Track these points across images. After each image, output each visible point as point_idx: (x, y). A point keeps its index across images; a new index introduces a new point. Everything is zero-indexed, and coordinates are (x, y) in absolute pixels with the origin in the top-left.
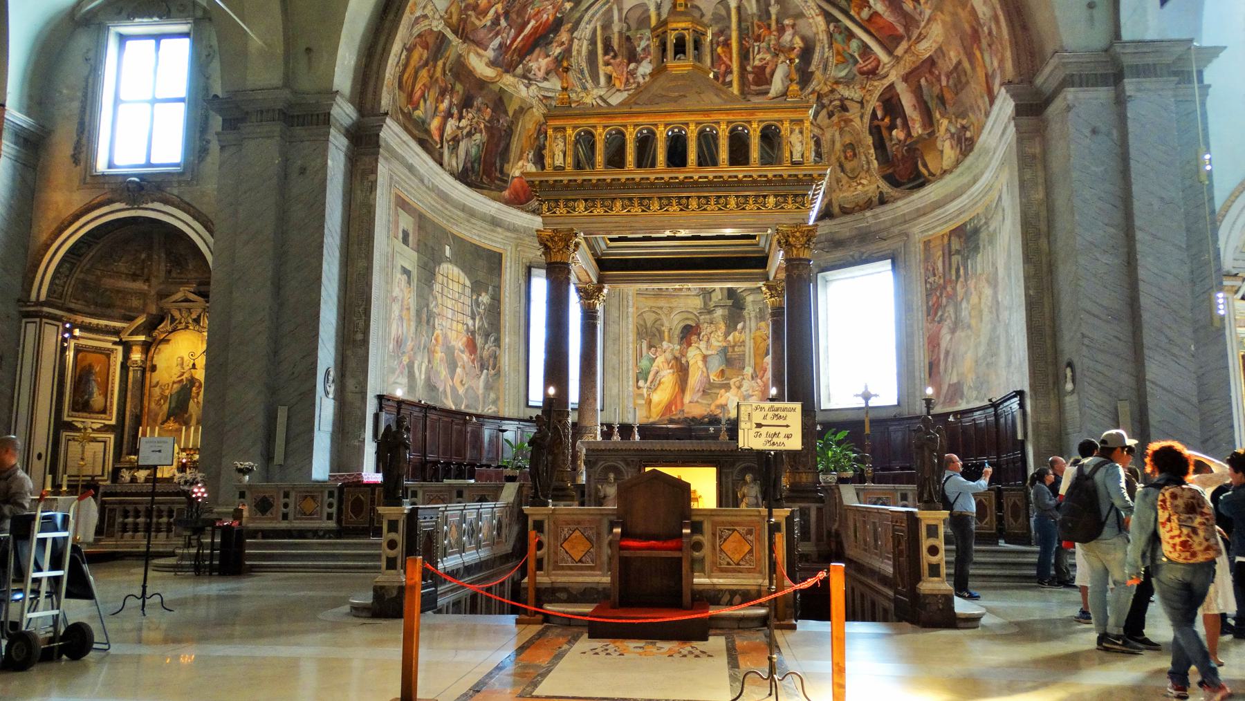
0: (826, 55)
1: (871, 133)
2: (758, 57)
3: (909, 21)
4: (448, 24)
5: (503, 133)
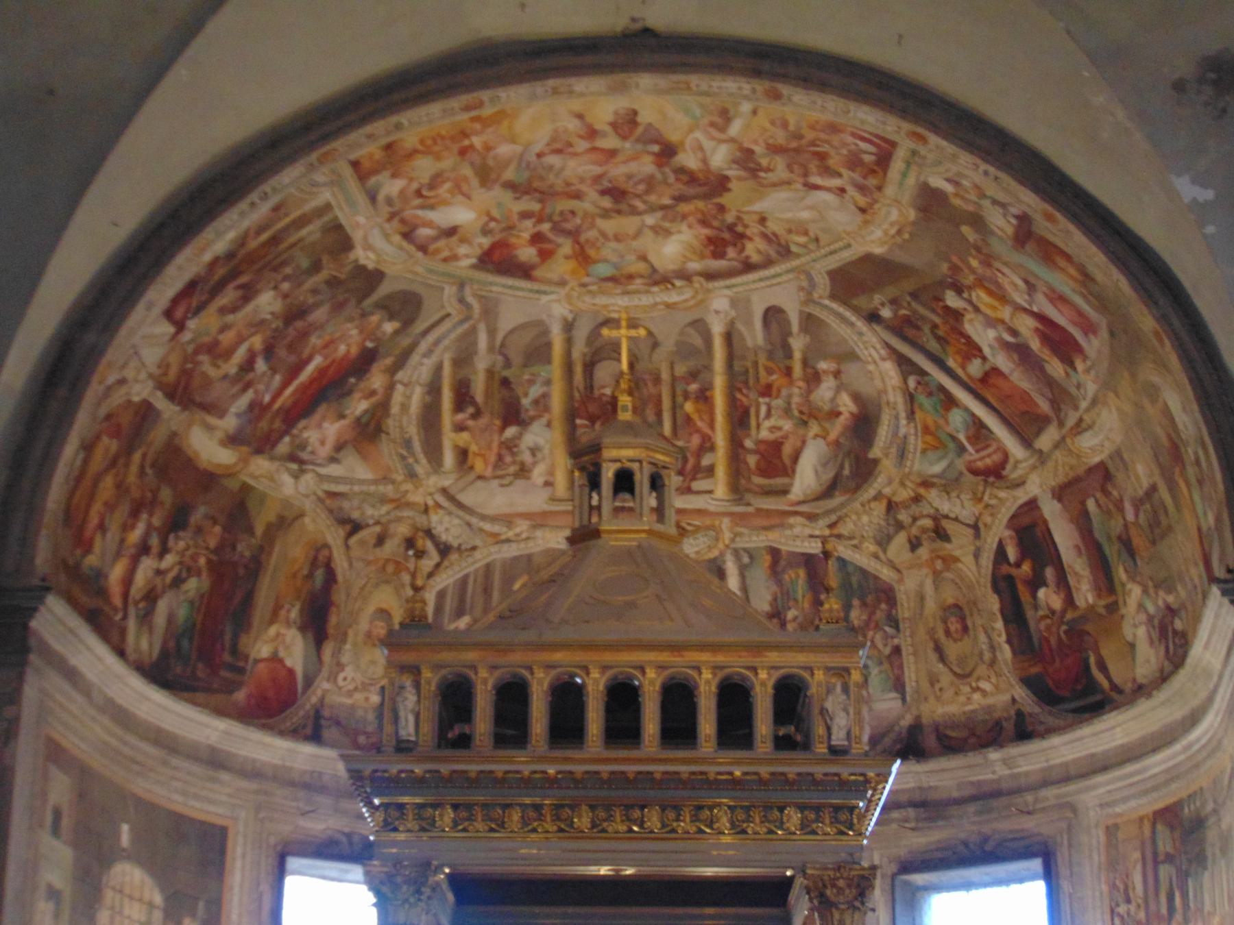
0: (903, 431)
1: (996, 588)
2: (767, 424)
3: (1060, 397)
4: (160, 386)
5: (241, 572)
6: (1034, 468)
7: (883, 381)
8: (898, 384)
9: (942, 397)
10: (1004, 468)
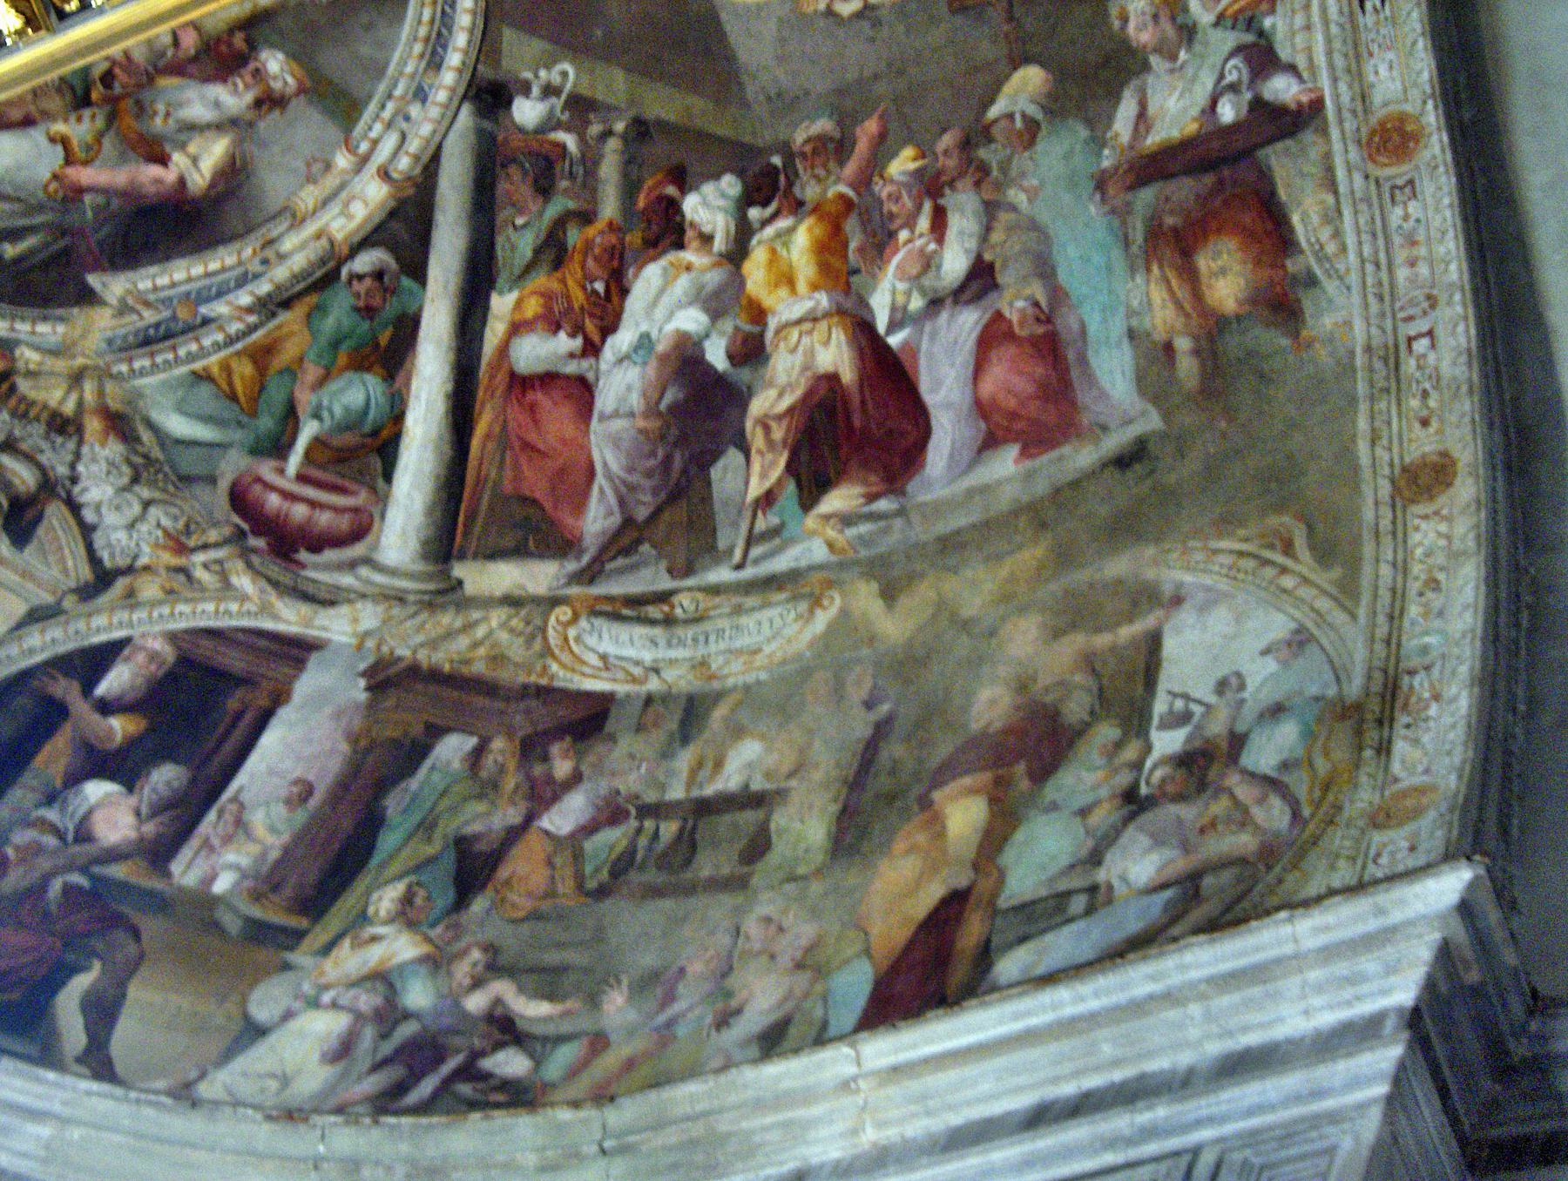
0: (220, 308)
6: (400, 598)
7: (325, 202)
8: (339, 236)
9: (384, 339)
10: (316, 548)
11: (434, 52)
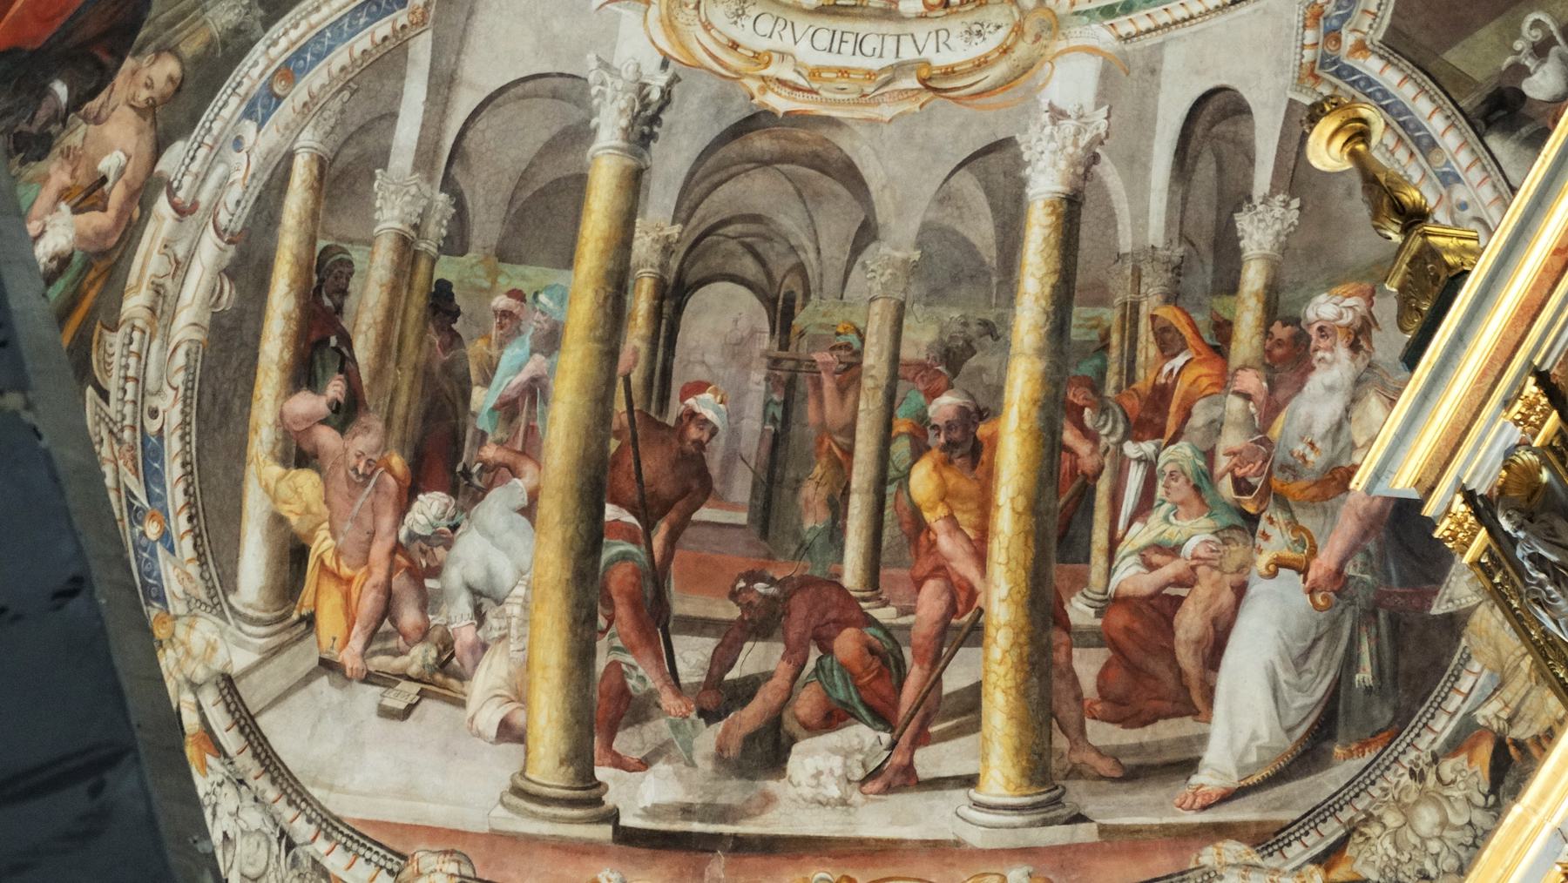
2: (1140, 535)
11: (1417, 141)
